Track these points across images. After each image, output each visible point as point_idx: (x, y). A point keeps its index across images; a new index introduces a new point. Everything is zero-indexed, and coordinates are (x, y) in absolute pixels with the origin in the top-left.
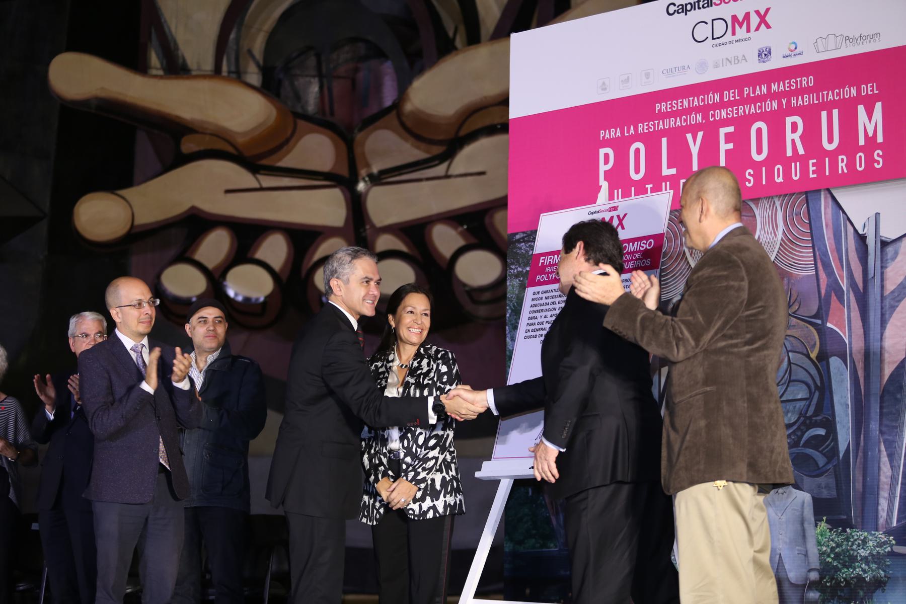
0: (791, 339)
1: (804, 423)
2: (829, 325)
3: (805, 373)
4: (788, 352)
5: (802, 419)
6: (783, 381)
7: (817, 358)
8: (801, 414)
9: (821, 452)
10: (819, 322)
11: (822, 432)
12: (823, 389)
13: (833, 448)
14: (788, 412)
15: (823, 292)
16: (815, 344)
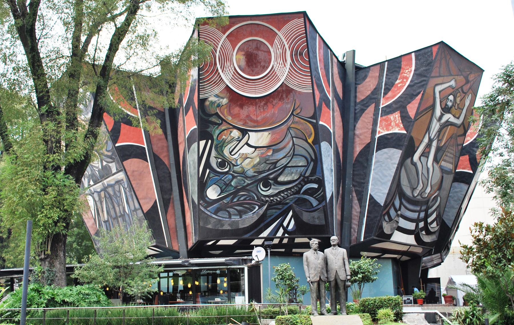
0: (295, 129)
2: (321, 123)
4: (292, 137)
5: (302, 178)
7: (312, 142)
9: (315, 198)
10: (314, 121)
11: (315, 186)
12: (316, 161)
13: (323, 195)
14: (292, 173)
15: (317, 103)
16: (312, 134)
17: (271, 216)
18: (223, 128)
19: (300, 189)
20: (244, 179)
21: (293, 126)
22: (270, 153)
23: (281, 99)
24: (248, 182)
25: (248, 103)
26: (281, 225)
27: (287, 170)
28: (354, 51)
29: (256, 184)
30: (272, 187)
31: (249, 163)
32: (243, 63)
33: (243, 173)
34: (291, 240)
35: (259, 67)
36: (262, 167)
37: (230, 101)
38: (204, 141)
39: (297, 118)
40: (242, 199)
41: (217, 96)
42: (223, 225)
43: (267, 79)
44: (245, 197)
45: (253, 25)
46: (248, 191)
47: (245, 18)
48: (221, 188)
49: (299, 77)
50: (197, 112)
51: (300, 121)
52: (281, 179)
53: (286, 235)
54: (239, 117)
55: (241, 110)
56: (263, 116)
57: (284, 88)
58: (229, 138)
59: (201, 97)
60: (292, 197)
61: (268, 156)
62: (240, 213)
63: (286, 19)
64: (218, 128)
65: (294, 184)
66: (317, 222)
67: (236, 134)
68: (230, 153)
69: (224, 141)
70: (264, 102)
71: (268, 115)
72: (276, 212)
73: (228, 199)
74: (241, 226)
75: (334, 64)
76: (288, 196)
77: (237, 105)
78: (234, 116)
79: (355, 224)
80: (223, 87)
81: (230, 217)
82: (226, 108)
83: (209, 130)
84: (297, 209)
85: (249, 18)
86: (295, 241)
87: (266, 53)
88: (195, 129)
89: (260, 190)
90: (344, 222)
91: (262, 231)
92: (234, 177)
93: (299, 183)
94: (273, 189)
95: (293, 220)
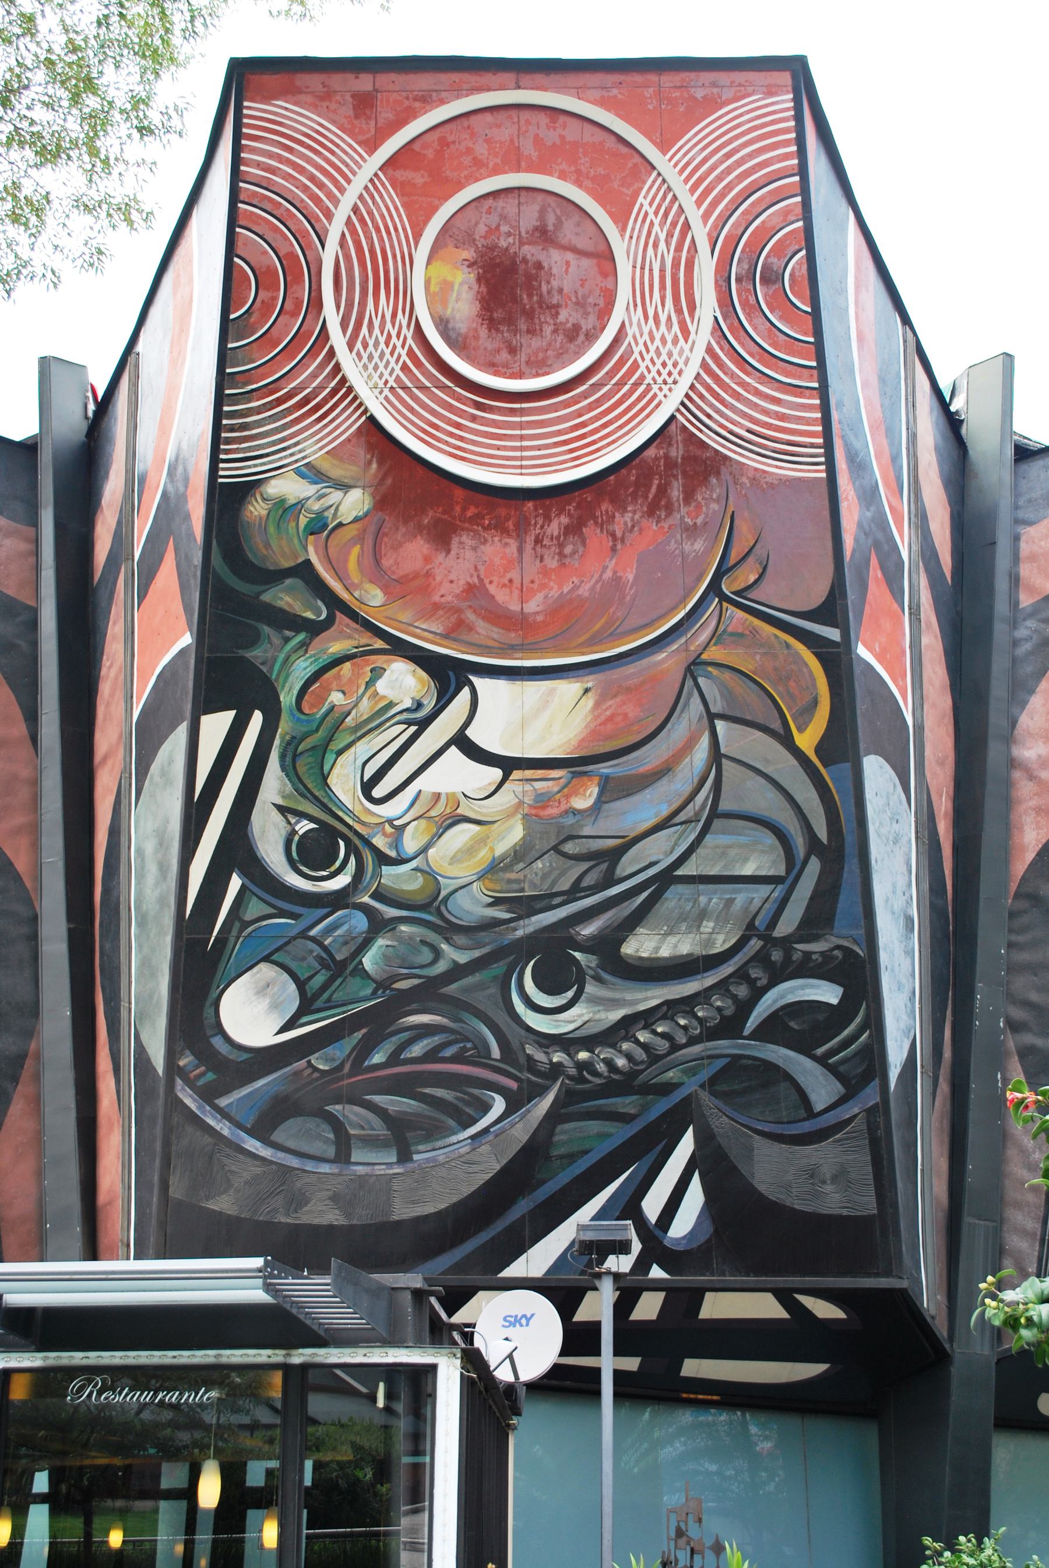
0: (727, 675)
1: (761, 958)
3: (772, 794)
4: (712, 717)
6: (688, 812)
7: (818, 750)
8: (751, 926)
9: (821, 1060)
10: (834, 634)
11: (829, 994)
12: (839, 852)
14: (703, 915)
16: (815, 703)
17: (572, 1158)
18: (337, 648)
19: (745, 1008)
20: (432, 937)
21: (714, 653)
22: (583, 802)
23: (659, 507)
24: (454, 954)
25: (477, 519)
26: (629, 1207)
27: (674, 898)
28: (1008, 358)
29: (498, 968)
30: (590, 988)
31: (469, 851)
32: (464, 307)
33: (431, 906)
34: (683, 1301)
35: (548, 330)
36: (539, 874)
37: (383, 502)
38: (228, 717)
39: (740, 614)
40: (417, 1050)
41: (312, 473)
42: (297, 1201)
43: (585, 395)
44: (436, 1040)
45: (525, 115)
46: (457, 1006)
47: (488, 78)
48: (301, 985)
49: (757, 393)
50: (197, 558)
51: (754, 631)
52: (641, 945)
53: (656, 1272)
54: (425, 590)
55: (441, 557)
56: (554, 593)
57: (677, 452)
58: (366, 707)
59: (227, 473)
60: (696, 1049)
61: (575, 812)
62: (402, 1136)
63: (699, 94)
64: (304, 645)
65: (710, 979)
66: (833, 1202)
67: (403, 682)
68: (367, 787)
69: (335, 721)
70: (564, 520)
71: (584, 591)
72: (603, 1136)
73: (341, 1050)
74: (403, 1211)
75: (918, 395)
76: (675, 1047)
77: (420, 528)
78: (398, 588)
79: (1024, 1233)
80: (345, 425)
81: (343, 1156)
82: (360, 539)
83: (256, 654)
84: (721, 1123)
85: (510, 77)
86: (705, 1313)
87: (586, 262)
88: (182, 652)
89: (520, 1007)
90: (968, 1220)
91: (518, 1244)
92: (378, 925)
93: (741, 975)
94: (595, 1001)
95: (695, 1186)
